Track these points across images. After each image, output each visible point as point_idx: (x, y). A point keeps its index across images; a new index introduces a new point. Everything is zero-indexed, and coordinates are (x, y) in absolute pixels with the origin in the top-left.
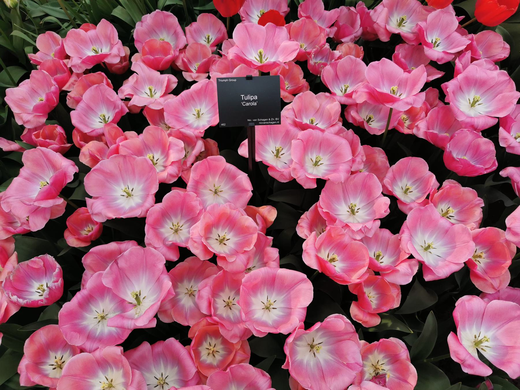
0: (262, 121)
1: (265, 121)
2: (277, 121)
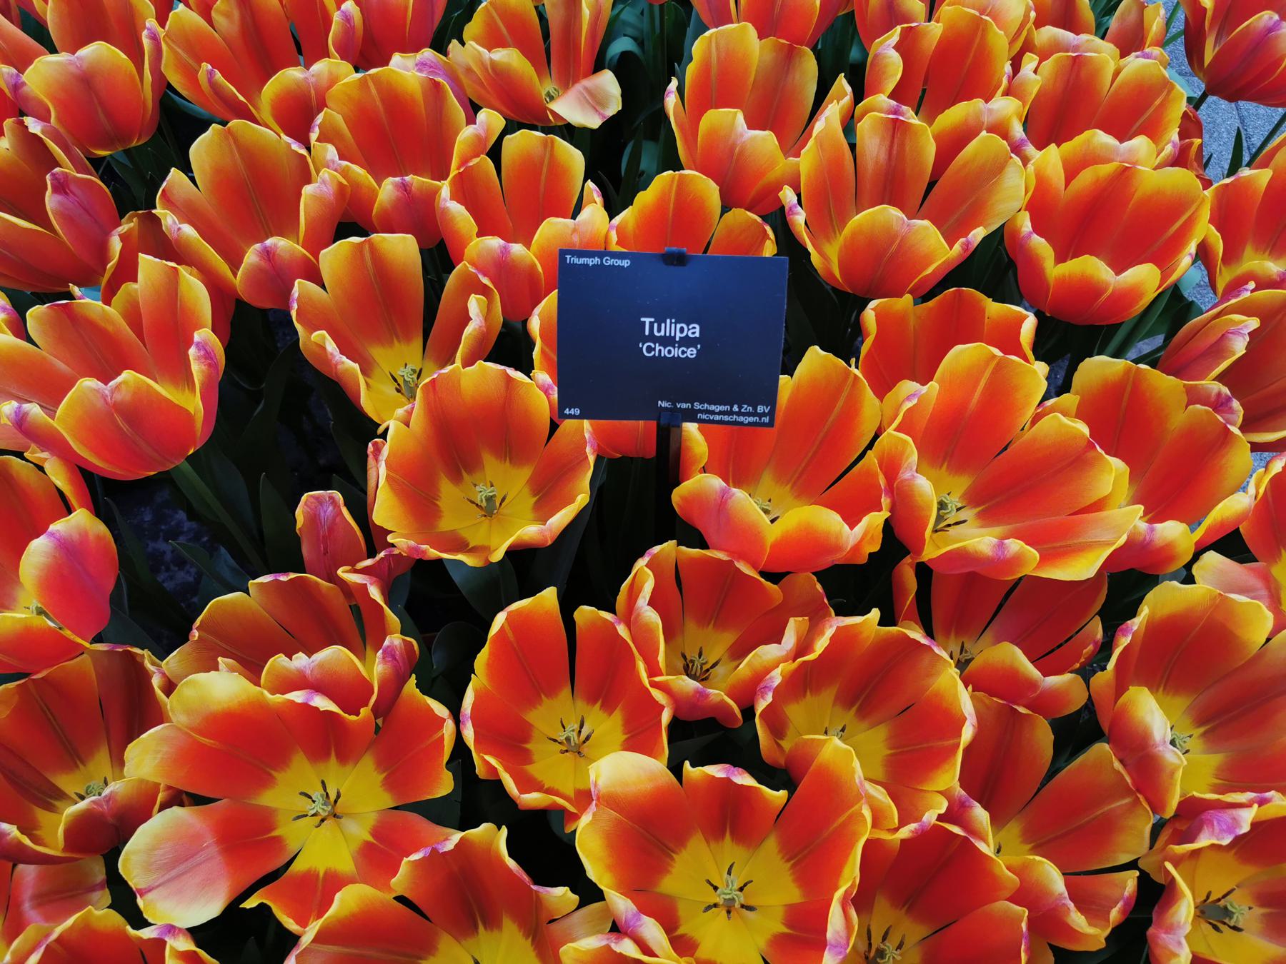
0: (707, 412)
1: (720, 413)
2: (764, 414)
